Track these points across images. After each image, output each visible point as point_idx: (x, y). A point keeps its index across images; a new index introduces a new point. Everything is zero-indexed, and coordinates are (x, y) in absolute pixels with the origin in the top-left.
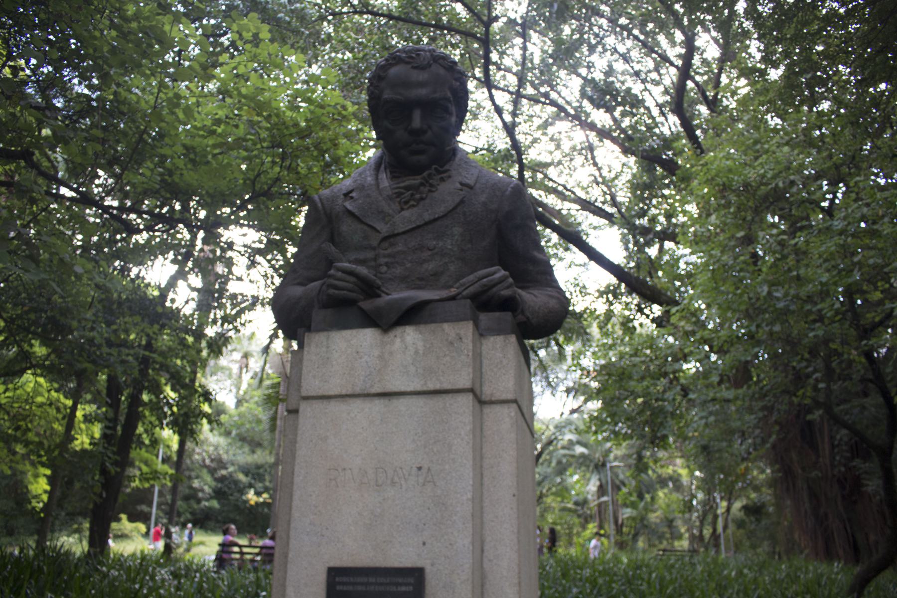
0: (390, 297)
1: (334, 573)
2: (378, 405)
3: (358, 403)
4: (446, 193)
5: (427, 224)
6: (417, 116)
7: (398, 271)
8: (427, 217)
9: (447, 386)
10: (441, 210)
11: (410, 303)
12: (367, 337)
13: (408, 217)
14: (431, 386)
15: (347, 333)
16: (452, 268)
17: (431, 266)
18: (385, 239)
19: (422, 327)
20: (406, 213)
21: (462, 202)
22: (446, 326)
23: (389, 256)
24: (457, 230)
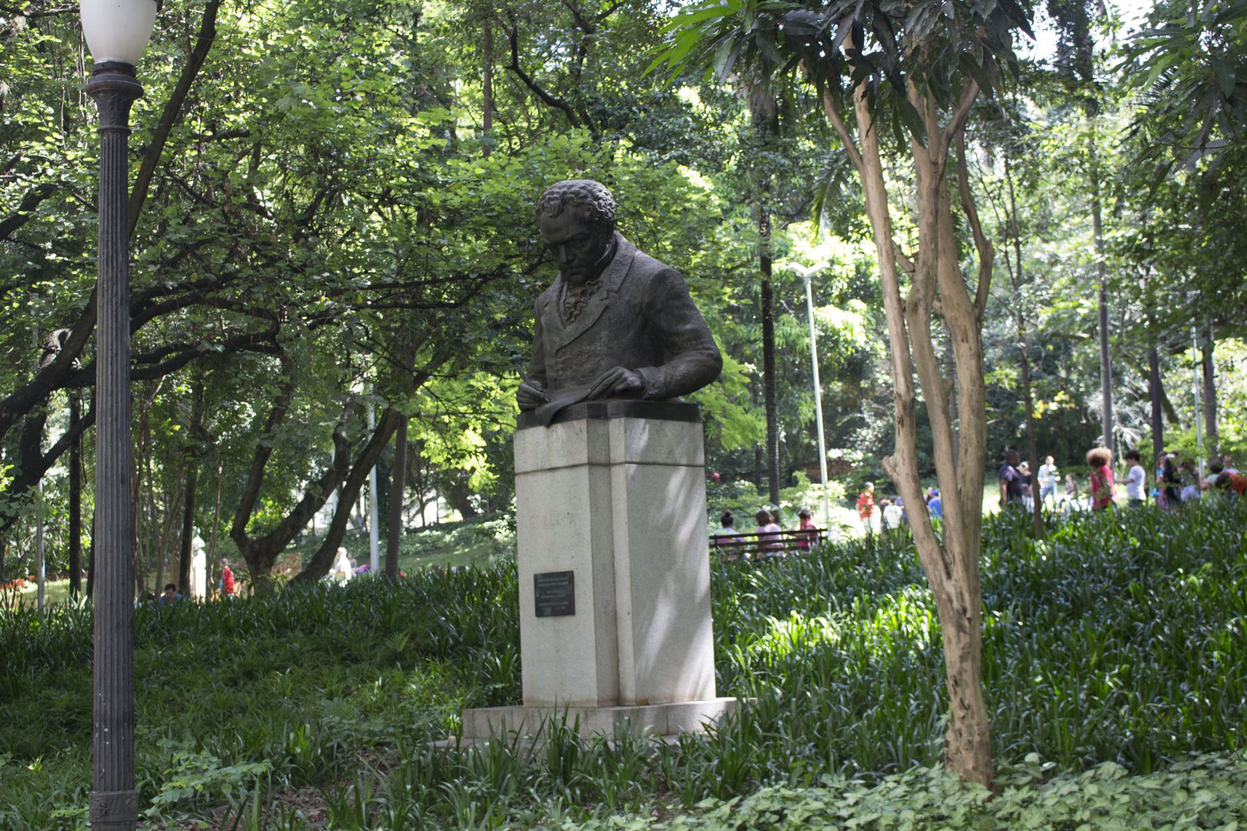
0: (548, 406)
1: (536, 577)
2: (548, 475)
3: (540, 476)
4: (594, 304)
5: (582, 334)
6: (562, 249)
7: (569, 373)
8: (581, 330)
9: (577, 462)
10: (589, 322)
11: (554, 411)
12: (541, 430)
13: (571, 330)
14: (571, 463)
15: (532, 430)
16: (603, 364)
17: (588, 366)
18: (558, 351)
19: (565, 424)
20: (569, 329)
21: (607, 308)
22: (575, 423)
23: (563, 362)
24: (604, 333)
